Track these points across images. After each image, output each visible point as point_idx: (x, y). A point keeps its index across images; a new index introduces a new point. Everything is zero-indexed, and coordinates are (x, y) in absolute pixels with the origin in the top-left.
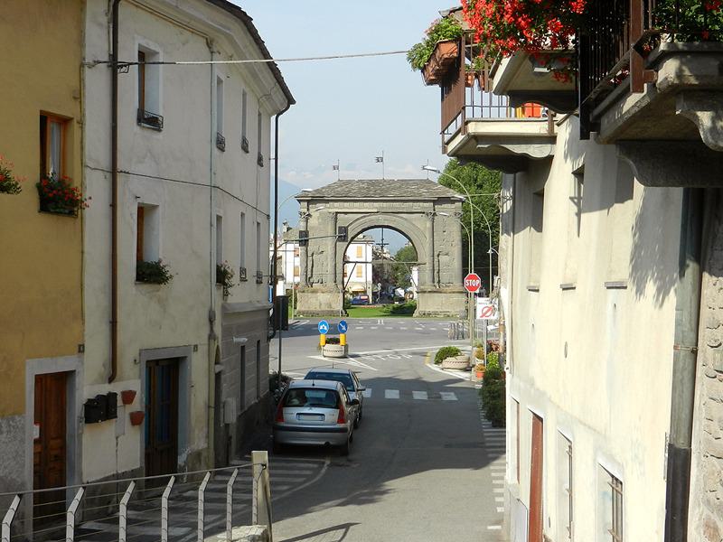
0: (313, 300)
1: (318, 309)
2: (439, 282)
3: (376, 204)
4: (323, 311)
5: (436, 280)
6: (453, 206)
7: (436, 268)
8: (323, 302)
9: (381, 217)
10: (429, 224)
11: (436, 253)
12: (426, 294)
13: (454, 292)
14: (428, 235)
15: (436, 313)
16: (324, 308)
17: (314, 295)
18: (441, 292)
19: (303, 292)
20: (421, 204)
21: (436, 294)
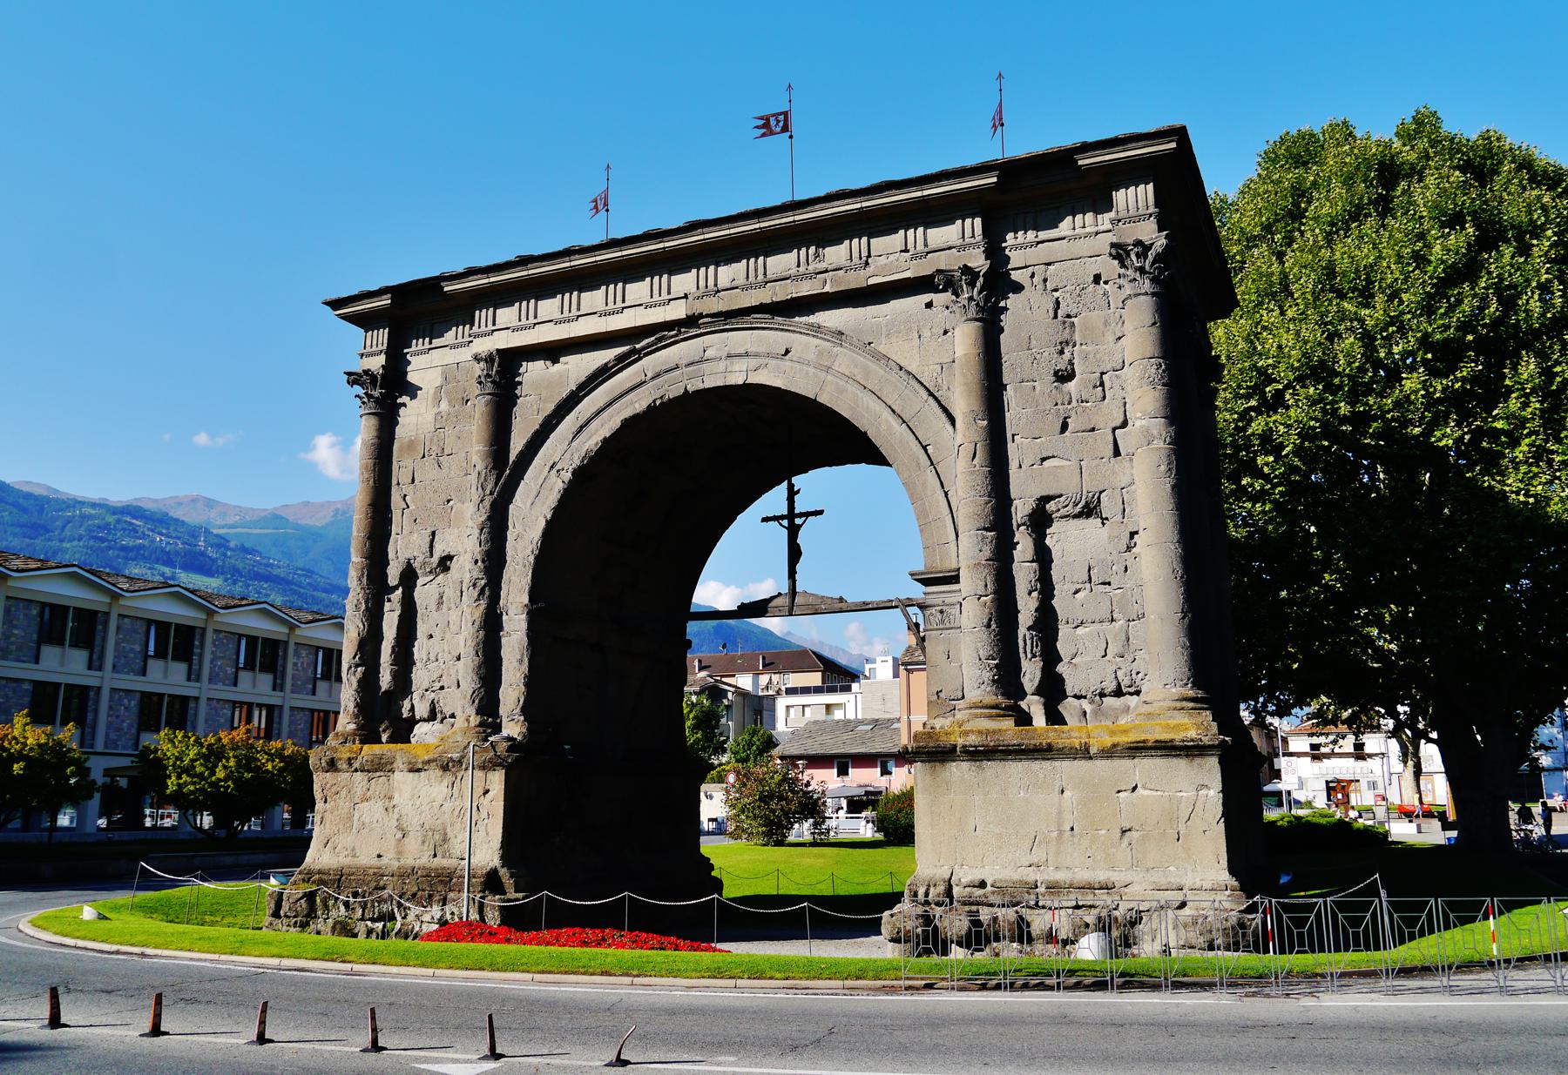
0: (371, 811)
1: (390, 862)
2: (1053, 689)
3: (684, 282)
4: (404, 874)
5: (1031, 673)
6: (1105, 220)
7: (1027, 607)
8: (413, 822)
9: (716, 343)
10: (965, 339)
11: (1021, 509)
12: (959, 770)
13: (1137, 749)
14: (964, 400)
15: (1020, 895)
16: (417, 855)
17: (379, 783)
18: (1044, 752)
19: (332, 766)
20: (916, 236)
21: (1016, 770)
